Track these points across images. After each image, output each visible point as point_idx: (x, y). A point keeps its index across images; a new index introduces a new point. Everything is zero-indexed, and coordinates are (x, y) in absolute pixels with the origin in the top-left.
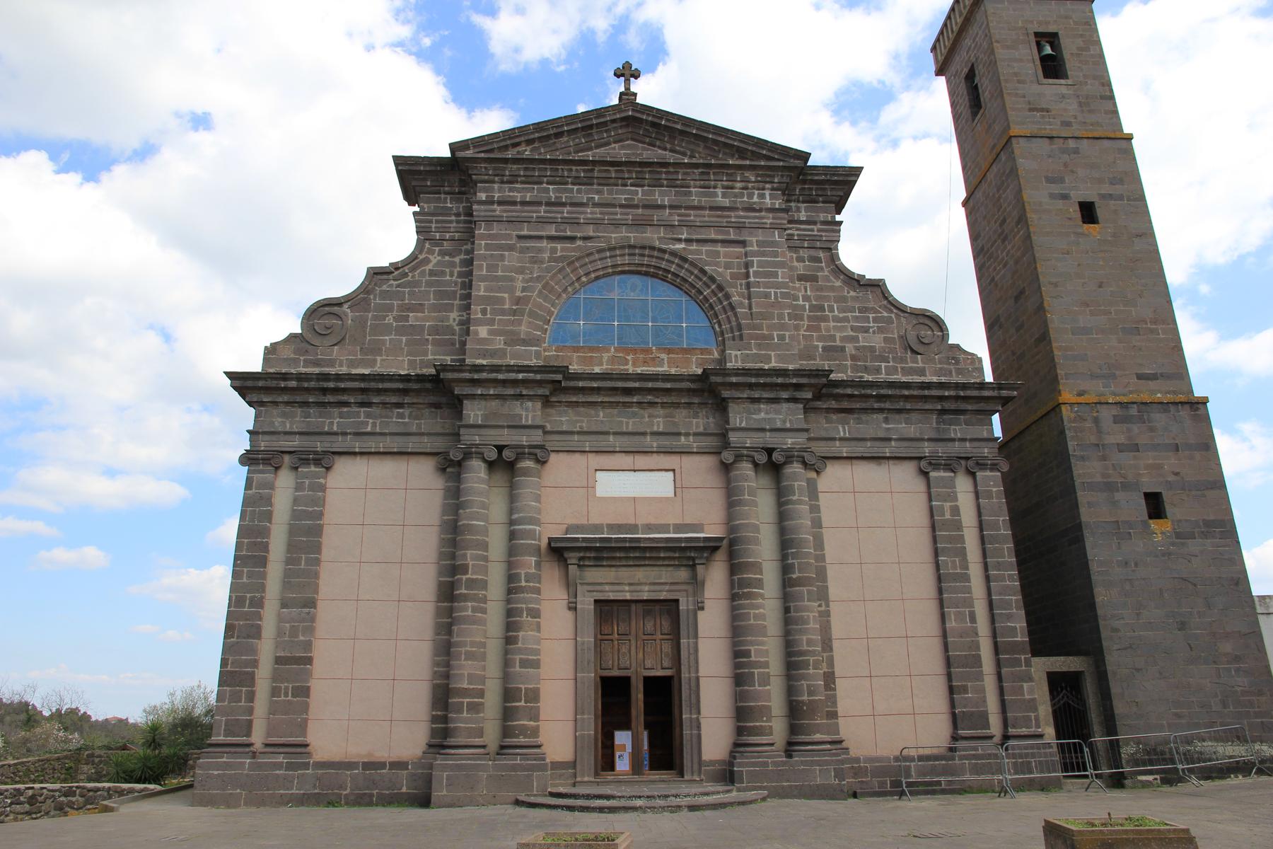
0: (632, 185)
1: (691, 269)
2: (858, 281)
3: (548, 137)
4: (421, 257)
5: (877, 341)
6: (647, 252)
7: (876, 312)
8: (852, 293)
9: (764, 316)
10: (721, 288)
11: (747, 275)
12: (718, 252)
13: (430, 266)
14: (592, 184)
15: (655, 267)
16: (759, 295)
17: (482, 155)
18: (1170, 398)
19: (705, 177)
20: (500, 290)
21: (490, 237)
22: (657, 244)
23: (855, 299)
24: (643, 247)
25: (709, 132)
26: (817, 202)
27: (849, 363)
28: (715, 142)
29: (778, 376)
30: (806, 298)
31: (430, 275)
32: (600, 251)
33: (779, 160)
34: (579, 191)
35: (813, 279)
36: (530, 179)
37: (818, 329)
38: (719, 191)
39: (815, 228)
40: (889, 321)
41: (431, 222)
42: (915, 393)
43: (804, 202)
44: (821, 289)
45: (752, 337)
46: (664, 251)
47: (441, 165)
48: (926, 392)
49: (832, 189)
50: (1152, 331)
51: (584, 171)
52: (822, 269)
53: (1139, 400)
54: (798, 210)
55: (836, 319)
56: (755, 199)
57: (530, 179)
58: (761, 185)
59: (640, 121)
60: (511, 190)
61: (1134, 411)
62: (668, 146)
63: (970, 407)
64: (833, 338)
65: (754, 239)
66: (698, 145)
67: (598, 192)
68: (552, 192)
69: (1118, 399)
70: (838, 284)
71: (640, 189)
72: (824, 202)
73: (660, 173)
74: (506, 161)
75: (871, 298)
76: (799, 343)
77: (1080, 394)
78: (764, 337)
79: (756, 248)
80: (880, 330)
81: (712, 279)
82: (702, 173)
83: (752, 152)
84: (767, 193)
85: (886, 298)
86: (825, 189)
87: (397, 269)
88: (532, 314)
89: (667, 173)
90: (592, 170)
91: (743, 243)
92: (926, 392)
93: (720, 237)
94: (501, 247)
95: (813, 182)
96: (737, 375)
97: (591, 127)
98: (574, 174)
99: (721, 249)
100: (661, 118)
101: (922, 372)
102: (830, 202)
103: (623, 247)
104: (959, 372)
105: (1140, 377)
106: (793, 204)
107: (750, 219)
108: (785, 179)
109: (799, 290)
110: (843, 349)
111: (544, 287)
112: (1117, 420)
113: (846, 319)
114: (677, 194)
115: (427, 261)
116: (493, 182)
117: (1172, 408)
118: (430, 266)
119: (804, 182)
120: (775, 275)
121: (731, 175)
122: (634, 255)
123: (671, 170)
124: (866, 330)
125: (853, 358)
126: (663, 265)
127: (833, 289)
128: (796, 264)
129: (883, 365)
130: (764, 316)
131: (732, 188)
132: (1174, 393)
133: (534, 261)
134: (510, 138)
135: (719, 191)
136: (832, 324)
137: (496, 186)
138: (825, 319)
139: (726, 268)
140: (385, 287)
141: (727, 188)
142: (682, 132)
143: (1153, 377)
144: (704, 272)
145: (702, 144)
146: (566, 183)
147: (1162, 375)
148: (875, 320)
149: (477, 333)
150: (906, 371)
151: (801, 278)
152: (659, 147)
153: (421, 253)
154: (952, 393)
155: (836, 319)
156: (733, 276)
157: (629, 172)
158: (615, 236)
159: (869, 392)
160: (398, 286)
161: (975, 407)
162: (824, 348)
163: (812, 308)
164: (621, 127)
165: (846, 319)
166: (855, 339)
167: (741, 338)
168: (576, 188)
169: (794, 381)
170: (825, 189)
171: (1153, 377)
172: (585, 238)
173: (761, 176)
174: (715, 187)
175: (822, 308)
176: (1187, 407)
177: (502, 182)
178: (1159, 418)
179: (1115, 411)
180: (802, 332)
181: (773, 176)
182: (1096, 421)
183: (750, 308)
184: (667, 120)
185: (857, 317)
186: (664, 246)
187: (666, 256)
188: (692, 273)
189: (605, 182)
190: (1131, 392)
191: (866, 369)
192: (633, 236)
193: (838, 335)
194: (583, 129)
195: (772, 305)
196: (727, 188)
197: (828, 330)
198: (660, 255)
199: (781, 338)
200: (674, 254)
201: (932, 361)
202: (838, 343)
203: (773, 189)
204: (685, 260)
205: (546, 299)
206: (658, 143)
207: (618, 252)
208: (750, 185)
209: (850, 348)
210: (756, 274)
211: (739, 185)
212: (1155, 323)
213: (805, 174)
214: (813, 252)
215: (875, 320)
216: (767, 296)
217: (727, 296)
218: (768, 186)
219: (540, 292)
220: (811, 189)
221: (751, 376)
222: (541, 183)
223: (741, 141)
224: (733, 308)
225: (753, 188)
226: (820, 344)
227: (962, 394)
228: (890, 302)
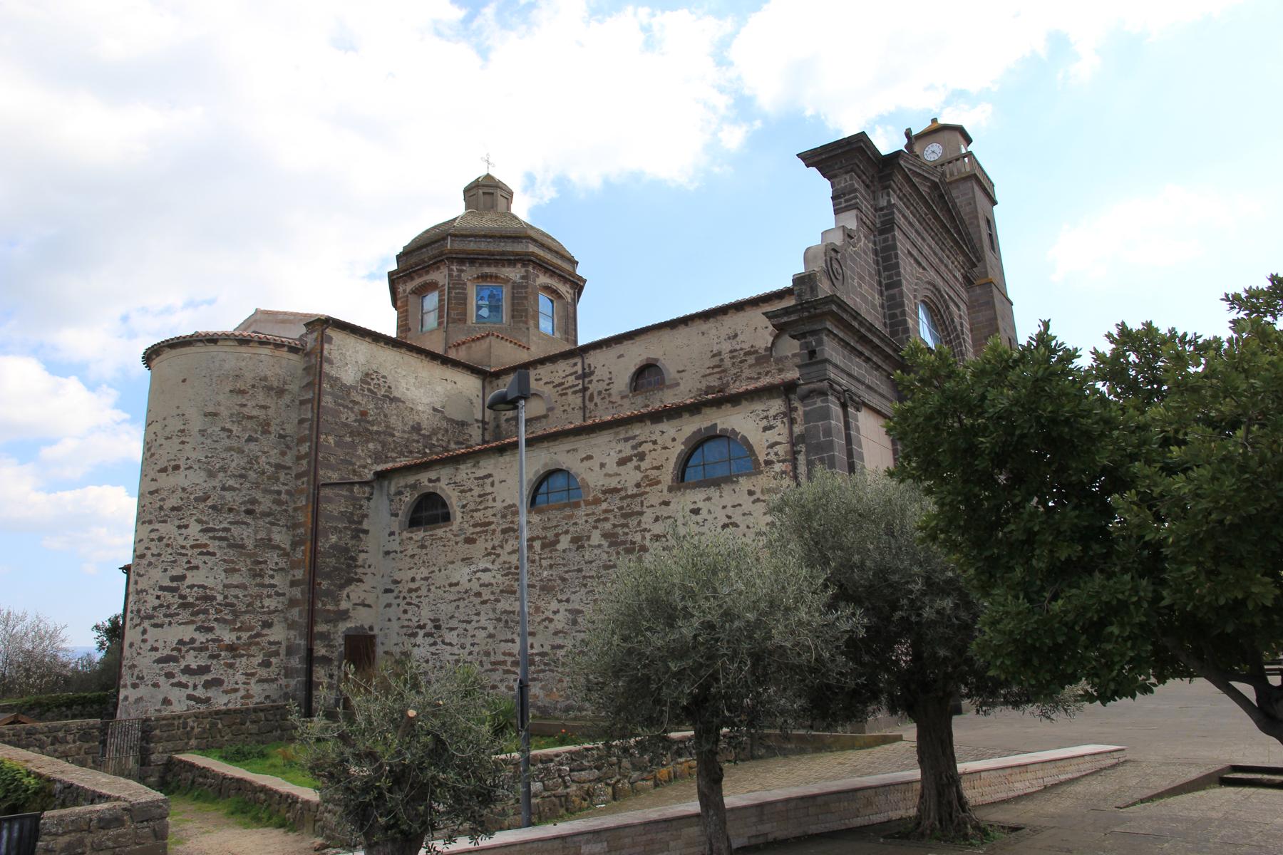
46: (942, 296)
200: (945, 301)
204: (948, 307)
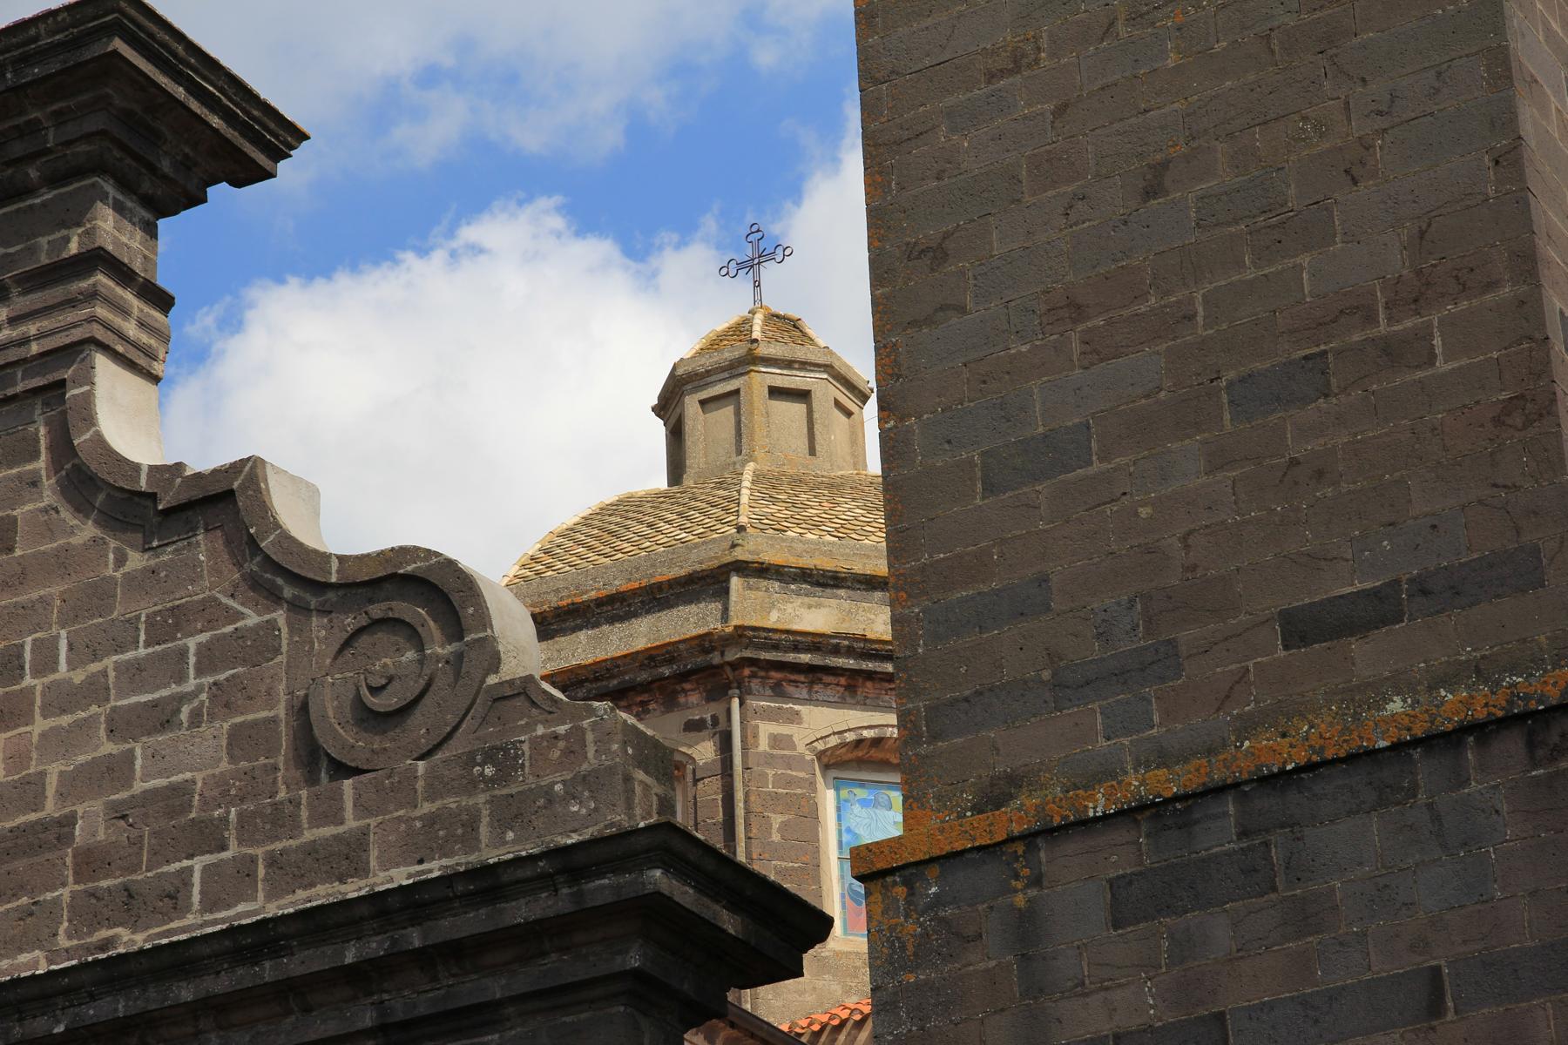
5: (198, 758)
8: (137, 561)
18: (1455, 704)
23: (138, 583)
26: (30, 191)
27: (65, 893)
40: (261, 645)
42: (220, 984)
48: (268, 971)
49: (60, 118)
50: (1392, 353)
53: (1244, 768)
61: (1219, 833)
63: (496, 988)
69: (1137, 784)
72: (54, 181)
77: (993, 798)
80: (224, 700)
86: (34, 128)
92: (268, 971)
101: (350, 855)
104: (510, 814)
105: (1300, 629)
112: (1127, 905)
117: (1426, 770)
124: (161, 718)
125: (91, 862)
132: (1479, 671)
143: (1376, 611)
147: (1422, 588)
150: (286, 871)
154: (375, 946)
161: (524, 980)
165: (95, 690)
166: (117, 770)
170: (34, 128)
171: (1376, 611)
176: (1511, 745)
178: (1350, 844)
179: (1122, 854)
182: (1026, 931)
190: (1247, 726)
191: (130, 905)
201: (404, 791)
202: (52, 808)
212: (1417, 303)
227: (415, 938)
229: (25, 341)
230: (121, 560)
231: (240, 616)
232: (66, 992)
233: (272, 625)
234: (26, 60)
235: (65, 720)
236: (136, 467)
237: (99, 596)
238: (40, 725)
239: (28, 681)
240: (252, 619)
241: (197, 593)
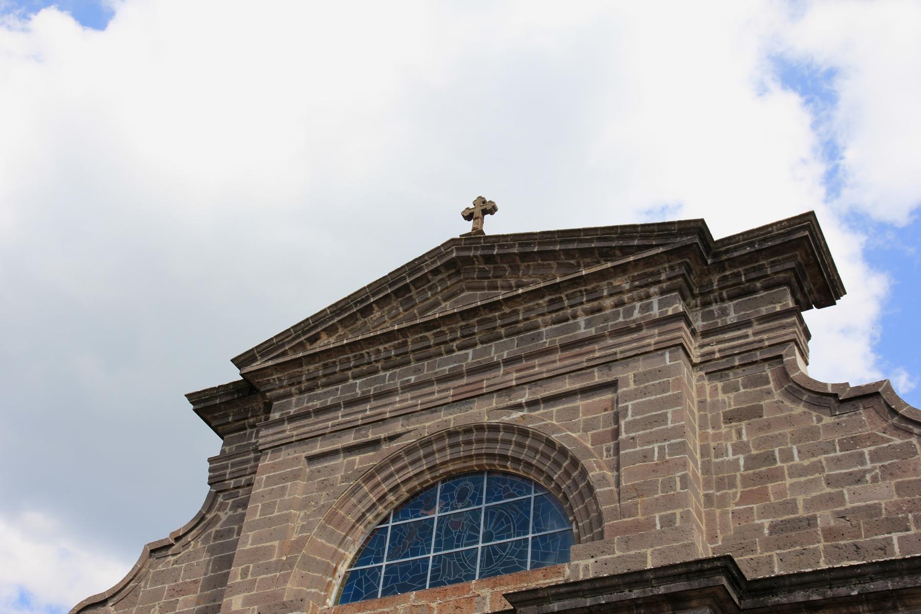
0: (460, 349)
1: (535, 444)
2: (835, 396)
3: (353, 317)
4: (209, 516)
6: (474, 436)
7: (872, 439)
8: (827, 420)
9: (638, 491)
10: (575, 463)
11: (616, 433)
12: (576, 409)
13: (218, 527)
14: (409, 363)
15: (479, 456)
16: (633, 458)
17: (270, 363)
19: (556, 307)
20: (271, 537)
21: (273, 467)
22: (485, 420)
24: (468, 431)
25: (555, 243)
26: (755, 292)
27: (821, 546)
28: (568, 253)
29: (631, 586)
30: (739, 448)
31: (215, 538)
32: (410, 450)
33: (658, 246)
34: (392, 377)
35: (755, 412)
36: (333, 378)
37: (762, 495)
38: (581, 320)
39: (750, 331)
41: (226, 467)
43: (731, 298)
44: (769, 426)
45: (616, 530)
47: (238, 391)
49: (773, 264)
51: (395, 347)
52: (769, 392)
54: (724, 312)
55: (797, 472)
56: (636, 314)
57: (333, 378)
58: (642, 292)
59: (469, 260)
60: (310, 399)
62: (513, 282)
64: (791, 506)
65: (631, 375)
66: (549, 267)
67: (417, 371)
68: (359, 387)
70: (800, 409)
71: (470, 351)
72: (766, 288)
73: (493, 320)
74: (298, 362)
75: (865, 420)
76: (724, 527)
78: (637, 526)
79: (632, 386)
81: (563, 452)
82: (551, 302)
83: (621, 248)
84: (655, 301)
85: (894, 412)
86: (762, 267)
87: (177, 539)
88: (307, 563)
89: (503, 317)
90: (405, 344)
91: (612, 385)
93: (577, 386)
94: (284, 478)
95: (733, 262)
96: (559, 597)
97: (406, 288)
98: (383, 355)
99: (580, 403)
100: (492, 247)
102: (779, 285)
103: (440, 438)
106: (715, 307)
107: (624, 345)
108: (677, 271)
109: (728, 437)
110: (811, 522)
111: (329, 520)
113: (817, 468)
114: (521, 342)
115: (216, 519)
116: (290, 395)
118: (218, 527)
119: (720, 266)
120: (663, 419)
121: (594, 290)
122: (457, 445)
123: (507, 310)
124: (858, 479)
125: (830, 534)
126: (498, 449)
127: (789, 420)
128: (721, 396)
129: (895, 536)
130: (638, 491)
131: (600, 310)
133: (323, 486)
134: (304, 333)
135: (581, 320)
136: (788, 481)
137: (294, 399)
138: (776, 476)
139: (585, 431)
140: (161, 568)
141: (593, 311)
142: (524, 256)
144: (550, 444)
145: (554, 264)
146: (376, 372)
148: (875, 457)
149: (229, 604)
151: (730, 418)
152: (503, 288)
153: (209, 511)
155: (797, 472)
156: (596, 441)
157: (452, 331)
158: (428, 425)
159: (842, 591)
160: (176, 562)
162: (773, 528)
163: (752, 462)
164: (450, 277)
165: (817, 468)
166: (838, 499)
167: (601, 536)
168: (388, 373)
169: (662, 590)
170: (762, 267)
172: (391, 438)
173: (640, 277)
174: (575, 317)
175: (769, 458)
177: (301, 392)
180: (732, 508)
181: (659, 273)
183: (618, 483)
184: (501, 247)
185: (838, 459)
186: (494, 421)
187: (501, 435)
188: (537, 451)
189: (425, 354)
192: (452, 418)
193: (800, 500)
194: (396, 293)
195: (655, 470)
196: (593, 311)
197: (780, 493)
198: (492, 435)
199: (668, 521)
200: (509, 428)
202: (801, 513)
203: (662, 292)
204: (524, 433)
205: (330, 536)
206: (499, 282)
207: (435, 447)
208: (625, 297)
209: (825, 518)
210: (631, 426)
211: (609, 302)
213: (716, 255)
214: (751, 371)
215: (875, 457)
216: (646, 456)
217: (584, 473)
218: (653, 290)
219: (323, 528)
220: (738, 275)
221: (584, 594)
222: (346, 380)
223: (599, 239)
224: (590, 488)
225: (633, 300)
226: (766, 522)
228: (904, 418)
229: (762, 341)
230: (820, 420)
231: (888, 440)
232: (858, 576)
233: (910, 444)
234: (765, 240)
235: (803, 479)
236: (825, 385)
237: (812, 433)
238: (788, 481)
239: (779, 464)
240: (897, 441)
241: (867, 430)
